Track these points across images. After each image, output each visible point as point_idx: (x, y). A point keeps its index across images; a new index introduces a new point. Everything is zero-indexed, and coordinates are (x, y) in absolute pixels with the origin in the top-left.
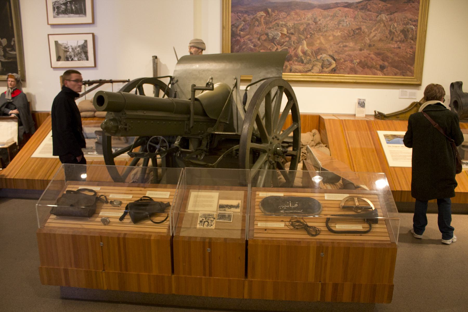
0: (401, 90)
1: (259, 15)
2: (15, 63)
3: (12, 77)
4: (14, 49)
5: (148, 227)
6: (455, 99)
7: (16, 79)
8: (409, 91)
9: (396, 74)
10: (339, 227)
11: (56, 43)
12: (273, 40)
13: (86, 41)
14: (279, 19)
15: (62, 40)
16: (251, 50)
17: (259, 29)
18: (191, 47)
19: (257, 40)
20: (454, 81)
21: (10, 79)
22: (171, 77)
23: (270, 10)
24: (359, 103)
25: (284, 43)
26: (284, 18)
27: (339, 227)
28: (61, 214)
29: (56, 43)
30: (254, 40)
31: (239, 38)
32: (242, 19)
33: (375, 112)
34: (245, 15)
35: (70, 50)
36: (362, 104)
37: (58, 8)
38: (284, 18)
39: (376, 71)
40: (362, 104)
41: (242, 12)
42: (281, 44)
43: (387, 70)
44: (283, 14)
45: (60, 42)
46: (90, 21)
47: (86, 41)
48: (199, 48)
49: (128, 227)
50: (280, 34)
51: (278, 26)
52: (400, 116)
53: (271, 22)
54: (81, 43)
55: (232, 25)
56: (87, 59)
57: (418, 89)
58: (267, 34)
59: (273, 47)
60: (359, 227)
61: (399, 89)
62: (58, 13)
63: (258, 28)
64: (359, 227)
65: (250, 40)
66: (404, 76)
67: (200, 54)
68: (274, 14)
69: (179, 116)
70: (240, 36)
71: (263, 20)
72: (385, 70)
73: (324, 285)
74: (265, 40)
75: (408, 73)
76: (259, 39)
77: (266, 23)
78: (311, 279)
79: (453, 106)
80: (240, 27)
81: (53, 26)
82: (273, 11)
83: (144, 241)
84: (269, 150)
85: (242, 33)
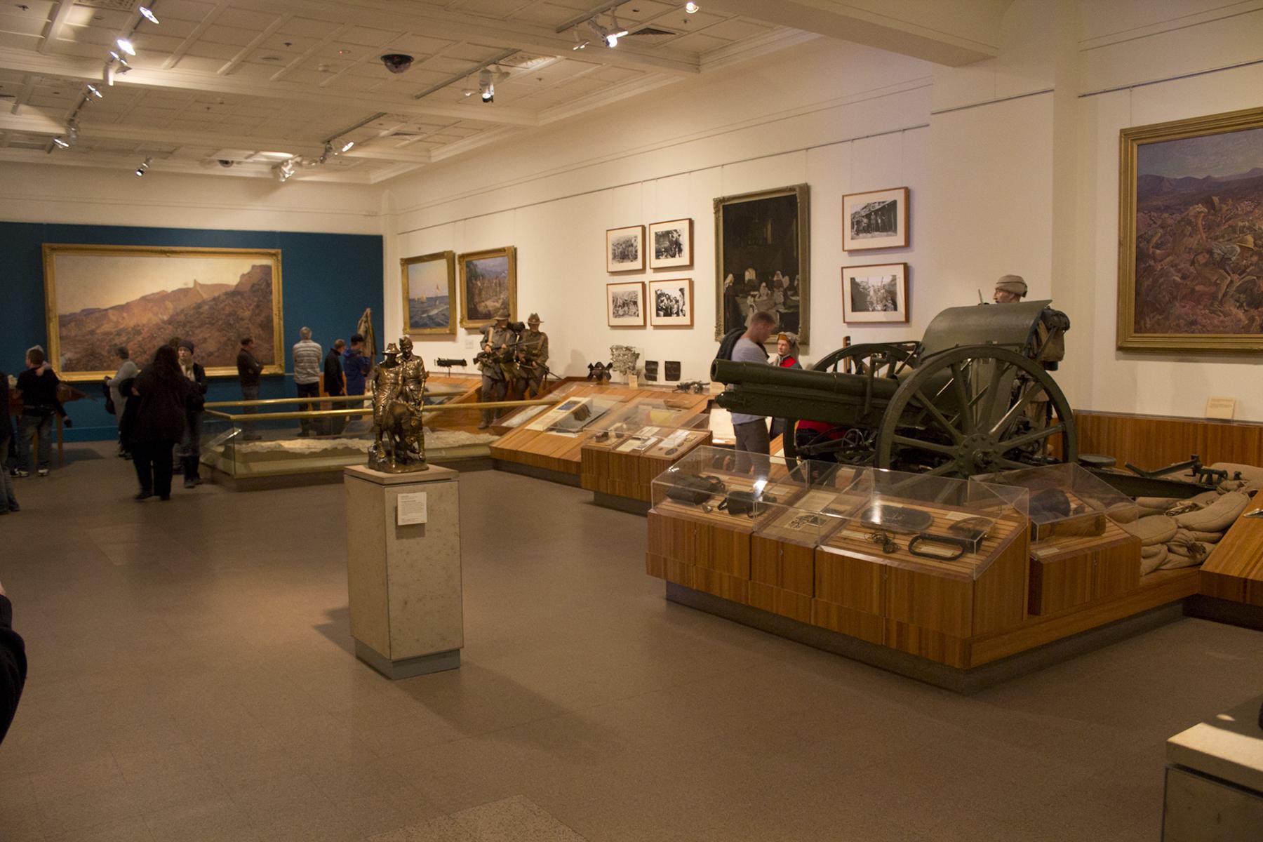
1: (1192, 213)
2: (796, 315)
3: (784, 337)
4: (796, 294)
5: (744, 522)
7: (789, 342)
10: (925, 549)
11: (853, 280)
12: (1222, 263)
13: (894, 278)
14: (1237, 216)
15: (861, 276)
16: (1177, 285)
17: (1193, 242)
18: (998, 290)
19: (1188, 265)
21: (781, 341)
22: (917, 343)
23: (1216, 199)
25: (1247, 267)
26: (1247, 213)
27: (925, 549)
28: (677, 497)
29: (853, 280)
30: (1182, 266)
31: (1152, 263)
32: (1159, 223)
34: (1166, 215)
35: (872, 293)
37: (858, 223)
38: (1247, 213)
41: (1157, 209)
42: (1242, 272)
44: (1246, 205)
45: (858, 280)
46: (902, 243)
47: (894, 278)
48: (1009, 292)
49: (725, 518)
50: (1238, 249)
51: (1235, 232)
53: (1218, 225)
54: (887, 280)
55: (1138, 238)
56: (895, 309)
58: (1210, 252)
59: (1224, 278)
60: (947, 553)
62: (858, 232)
63: (1191, 240)
64: (947, 553)
65: (1174, 266)
67: (1014, 302)
68: (1225, 207)
69: (846, 398)
70: (1154, 258)
71: (1200, 223)
73: (887, 621)
74: (1205, 265)
76: (1193, 263)
77: (1209, 228)
78: (876, 611)
80: (1155, 240)
81: (852, 252)
82: (1223, 200)
83: (728, 532)
84: (961, 456)
85: (1158, 251)
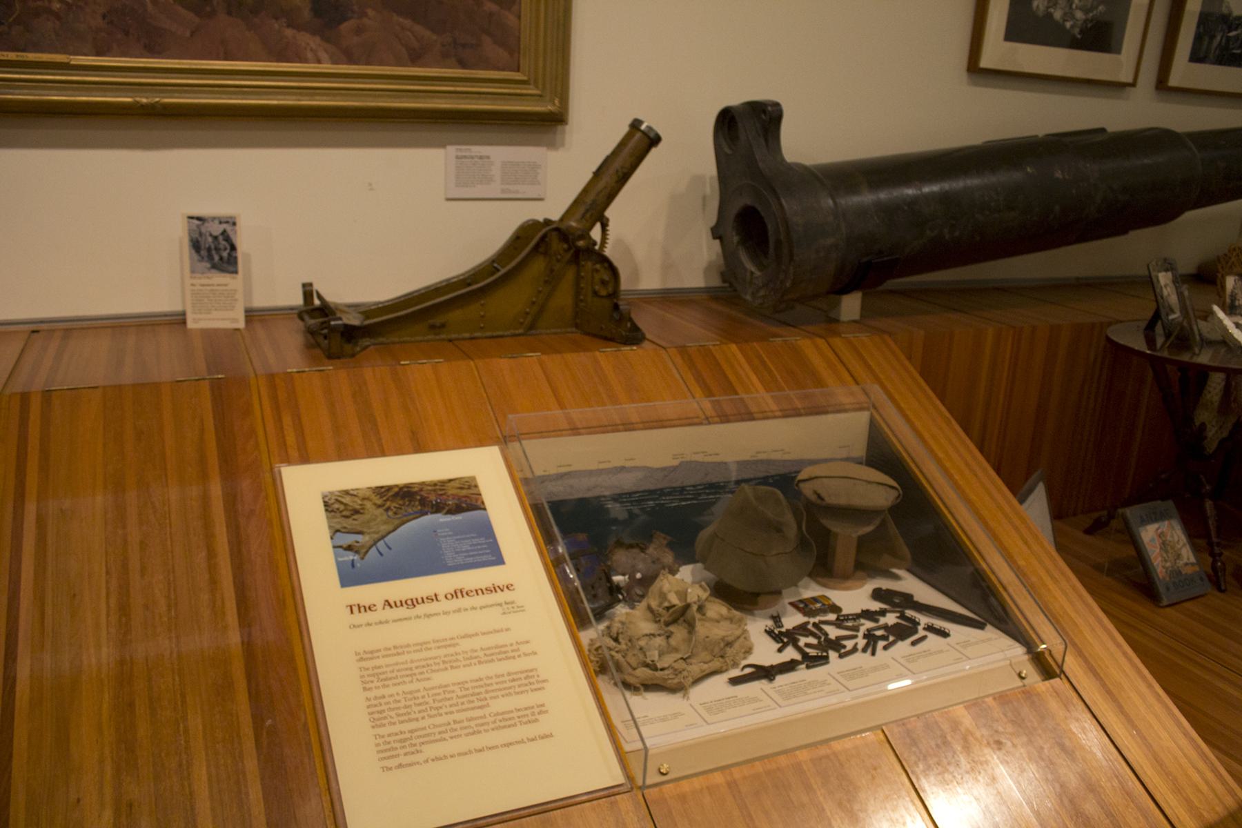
0: (452, 150)
6: (747, 200)
8: (501, 155)
9: (415, 58)
20: (735, 99)
24: (196, 245)
33: (308, 291)
36: (215, 248)
39: (289, 32)
40: (215, 248)
43: (359, 31)
52: (455, 316)
57: (552, 145)
61: (443, 146)
66: (463, 64)
72: (345, 27)
75: (490, 48)
79: (736, 239)
